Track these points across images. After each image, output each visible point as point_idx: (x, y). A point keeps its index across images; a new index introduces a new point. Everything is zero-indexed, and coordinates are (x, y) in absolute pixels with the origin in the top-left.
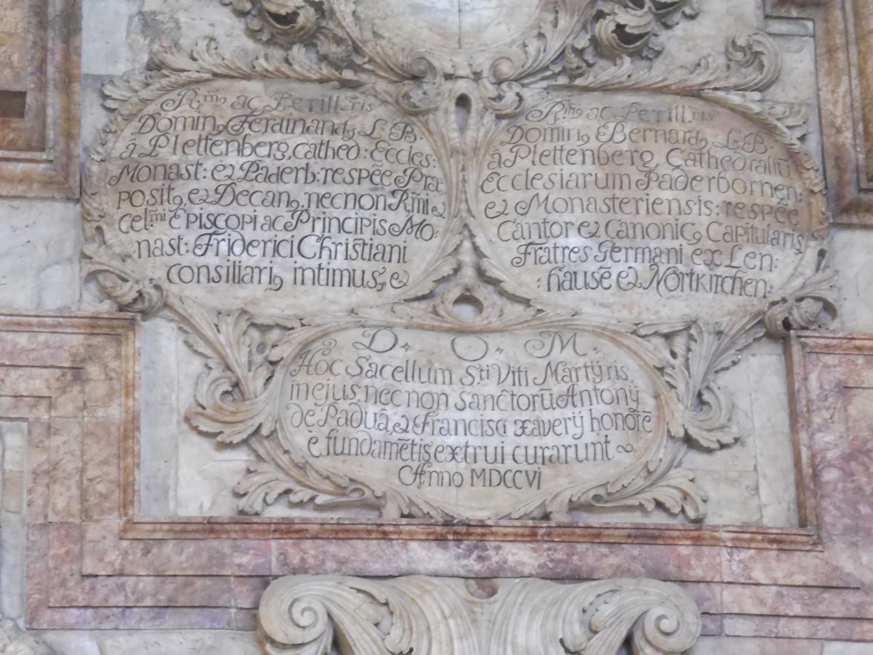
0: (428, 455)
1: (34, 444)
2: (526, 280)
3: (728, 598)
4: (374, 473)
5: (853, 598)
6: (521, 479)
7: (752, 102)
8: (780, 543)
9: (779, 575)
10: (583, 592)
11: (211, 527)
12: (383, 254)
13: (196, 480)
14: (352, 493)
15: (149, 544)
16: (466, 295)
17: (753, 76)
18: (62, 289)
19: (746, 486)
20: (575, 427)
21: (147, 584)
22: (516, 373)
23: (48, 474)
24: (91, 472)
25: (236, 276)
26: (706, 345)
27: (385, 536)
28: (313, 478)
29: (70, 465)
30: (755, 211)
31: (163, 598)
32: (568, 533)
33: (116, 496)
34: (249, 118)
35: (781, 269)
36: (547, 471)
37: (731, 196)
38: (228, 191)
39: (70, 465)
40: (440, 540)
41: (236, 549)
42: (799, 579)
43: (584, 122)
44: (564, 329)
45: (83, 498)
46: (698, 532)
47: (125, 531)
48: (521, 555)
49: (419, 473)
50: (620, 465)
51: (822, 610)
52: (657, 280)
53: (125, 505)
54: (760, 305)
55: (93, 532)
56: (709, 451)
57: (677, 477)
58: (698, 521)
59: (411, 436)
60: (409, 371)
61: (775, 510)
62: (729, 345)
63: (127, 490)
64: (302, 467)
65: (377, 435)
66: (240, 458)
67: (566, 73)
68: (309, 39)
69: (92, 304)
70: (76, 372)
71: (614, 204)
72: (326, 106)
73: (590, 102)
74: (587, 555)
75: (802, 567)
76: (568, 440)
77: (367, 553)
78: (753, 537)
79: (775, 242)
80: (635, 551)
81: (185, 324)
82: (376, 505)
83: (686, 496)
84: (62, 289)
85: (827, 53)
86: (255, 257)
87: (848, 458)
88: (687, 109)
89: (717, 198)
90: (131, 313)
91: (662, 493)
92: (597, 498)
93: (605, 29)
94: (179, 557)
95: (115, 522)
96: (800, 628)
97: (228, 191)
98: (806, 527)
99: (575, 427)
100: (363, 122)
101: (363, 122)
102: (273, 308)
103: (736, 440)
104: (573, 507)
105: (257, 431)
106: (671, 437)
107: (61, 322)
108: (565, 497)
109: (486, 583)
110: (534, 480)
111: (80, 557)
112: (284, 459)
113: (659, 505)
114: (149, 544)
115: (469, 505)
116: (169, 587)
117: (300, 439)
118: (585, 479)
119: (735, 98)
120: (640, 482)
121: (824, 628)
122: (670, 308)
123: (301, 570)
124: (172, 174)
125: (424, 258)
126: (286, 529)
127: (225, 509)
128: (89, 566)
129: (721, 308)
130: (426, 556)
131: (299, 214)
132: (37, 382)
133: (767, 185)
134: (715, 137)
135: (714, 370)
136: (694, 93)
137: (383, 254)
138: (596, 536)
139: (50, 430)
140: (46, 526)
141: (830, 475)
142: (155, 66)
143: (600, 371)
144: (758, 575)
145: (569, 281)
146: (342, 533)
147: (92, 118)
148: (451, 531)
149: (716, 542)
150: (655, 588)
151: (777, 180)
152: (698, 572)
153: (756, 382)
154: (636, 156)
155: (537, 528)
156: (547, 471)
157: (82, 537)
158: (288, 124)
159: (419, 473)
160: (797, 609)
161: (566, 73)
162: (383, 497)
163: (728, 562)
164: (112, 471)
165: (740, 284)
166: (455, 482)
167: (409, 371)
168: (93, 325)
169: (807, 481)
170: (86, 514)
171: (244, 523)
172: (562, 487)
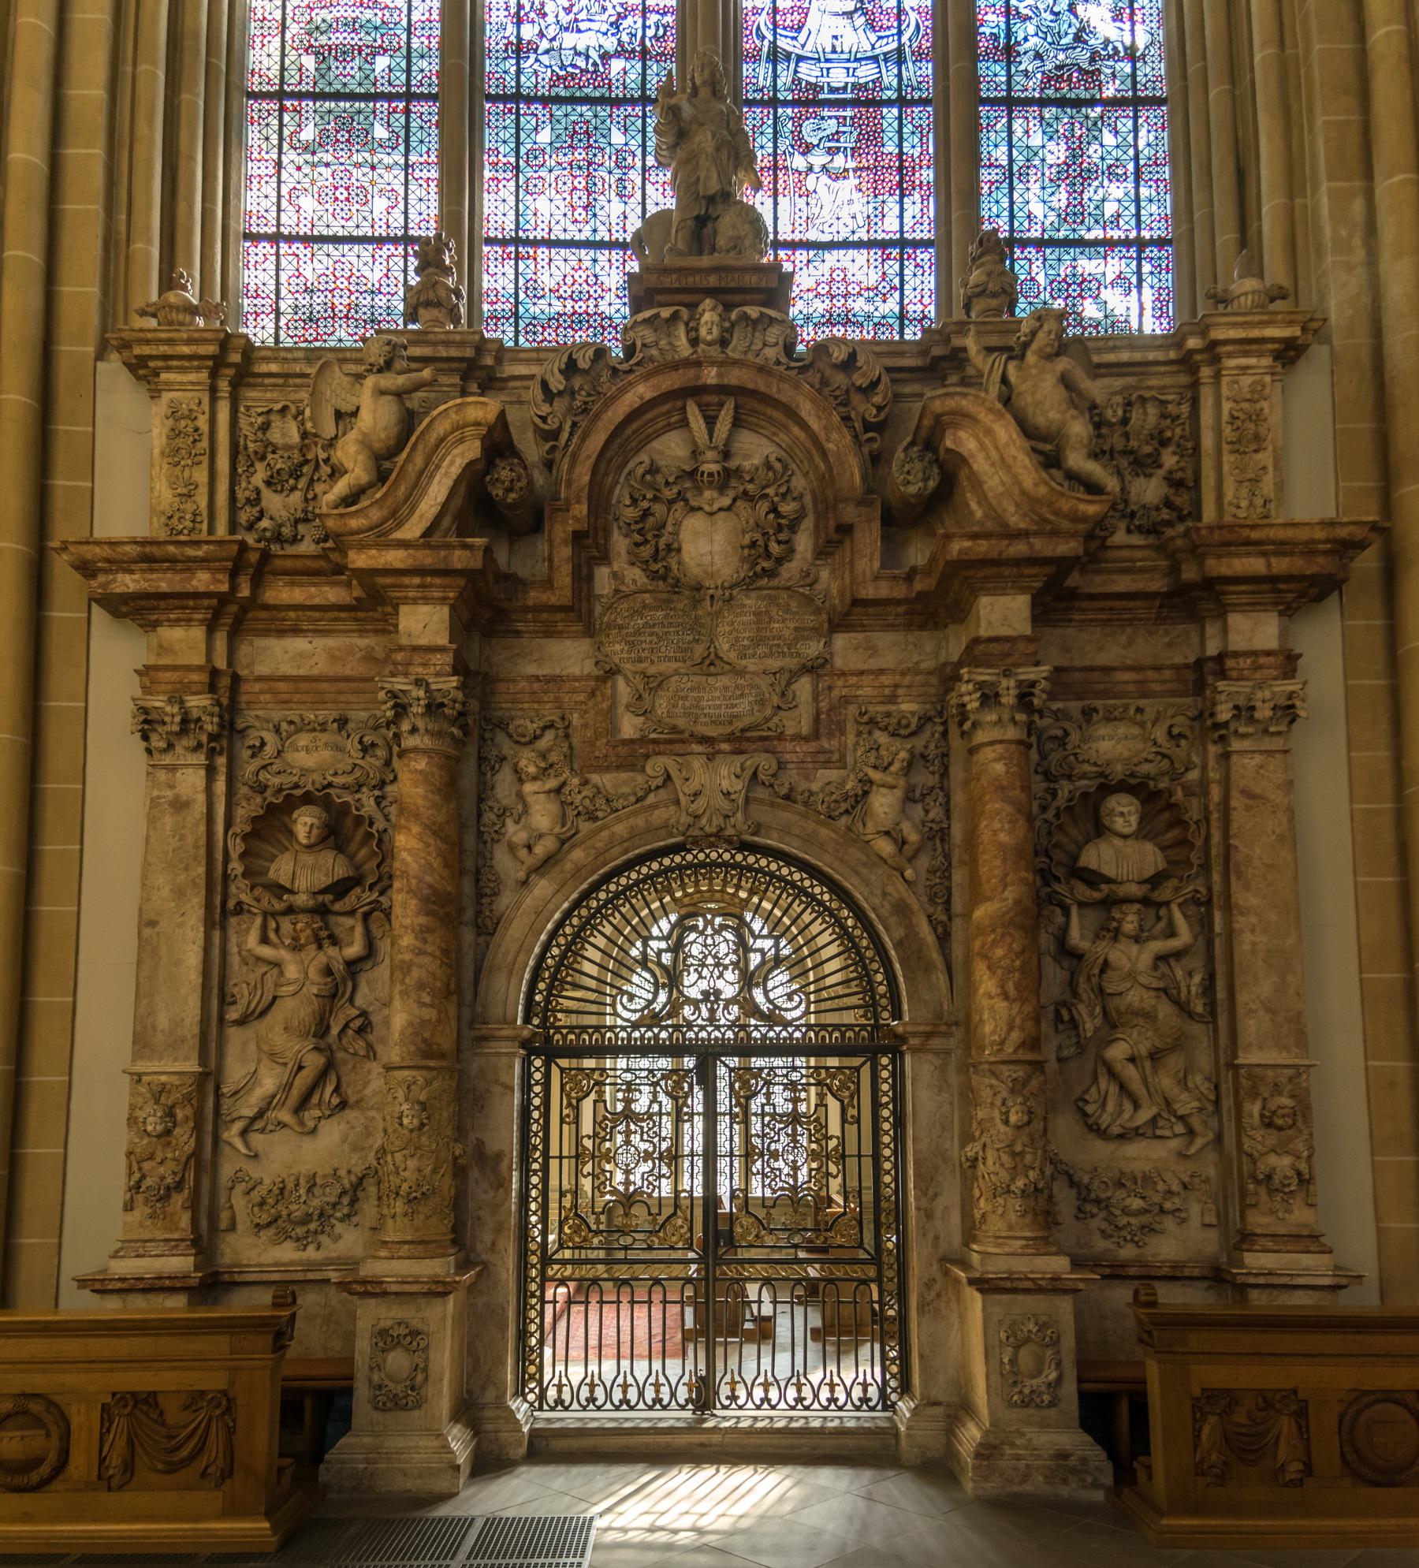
0: (697, 716)
2: (732, 656)
3: (788, 757)
4: (681, 722)
7: (806, 591)
8: (806, 739)
10: (741, 758)
11: (632, 741)
12: (685, 650)
13: (629, 727)
14: (674, 729)
16: (711, 663)
17: (808, 581)
18: (589, 667)
19: (800, 721)
20: (743, 705)
22: (726, 688)
23: (585, 726)
25: (640, 661)
26: (787, 675)
30: (804, 629)
32: (741, 739)
34: (645, 606)
35: (813, 648)
38: (638, 632)
43: (751, 602)
44: (741, 673)
46: (781, 737)
48: (725, 747)
50: (758, 717)
52: (772, 654)
57: (775, 719)
60: (691, 689)
61: (805, 730)
62: (795, 675)
67: (747, 584)
68: (664, 578)
69: (597, 672)
70: (593, 694)
71: (759, 630)
72: (670, 601)
73: (754, 594)
74: (745, 745)
75: (812, 746)
77: (678, 747)
78: (798, 738)
81: (626, 677)
82: (682, 732)
84: (589, 667)
85: (833, 571)
86: (646, 654)
88: (785, 595)
90: (612, 673)
91: (771, 724)
93: (758, 568)
94: (623, 751)
97: (638, 632)
98: (816, 735)
99: (743, 705)
100: (681, 606)
101: (681, 606)
102: (652, 670)
104: (743, 730)
107: (589, 677)
109: (710, 757)
115: (711, 732)
118: (747, 721)
122: (774, 664)
124: (621, 627)
125: (699, 650)
126: (655, 741)
127: (637, 736)
129: (792, 663)
130: (696, 748)
131: (660, 638)
132: (581, 697)
133: (809, 620)
134: (793, 604)
135: (789, 684)
136: (788, 588)
137: (685, 650)
138: (748, 739)
142: (617, 591)
143: (752, 686)
145: (743, 657)
146: (670, 742)
147: (598, 609)
148: (704, 740)
153: (803, 687)
154: (767, 612)
155: (729, 738)
158: (656, 608)
161: (747, 584)
163: (789, 746)
165: (798, 654)
167: (691, 689)
168: (597, 678)
169: (817, 719)
171: (643, 740)
172: (739, 725)
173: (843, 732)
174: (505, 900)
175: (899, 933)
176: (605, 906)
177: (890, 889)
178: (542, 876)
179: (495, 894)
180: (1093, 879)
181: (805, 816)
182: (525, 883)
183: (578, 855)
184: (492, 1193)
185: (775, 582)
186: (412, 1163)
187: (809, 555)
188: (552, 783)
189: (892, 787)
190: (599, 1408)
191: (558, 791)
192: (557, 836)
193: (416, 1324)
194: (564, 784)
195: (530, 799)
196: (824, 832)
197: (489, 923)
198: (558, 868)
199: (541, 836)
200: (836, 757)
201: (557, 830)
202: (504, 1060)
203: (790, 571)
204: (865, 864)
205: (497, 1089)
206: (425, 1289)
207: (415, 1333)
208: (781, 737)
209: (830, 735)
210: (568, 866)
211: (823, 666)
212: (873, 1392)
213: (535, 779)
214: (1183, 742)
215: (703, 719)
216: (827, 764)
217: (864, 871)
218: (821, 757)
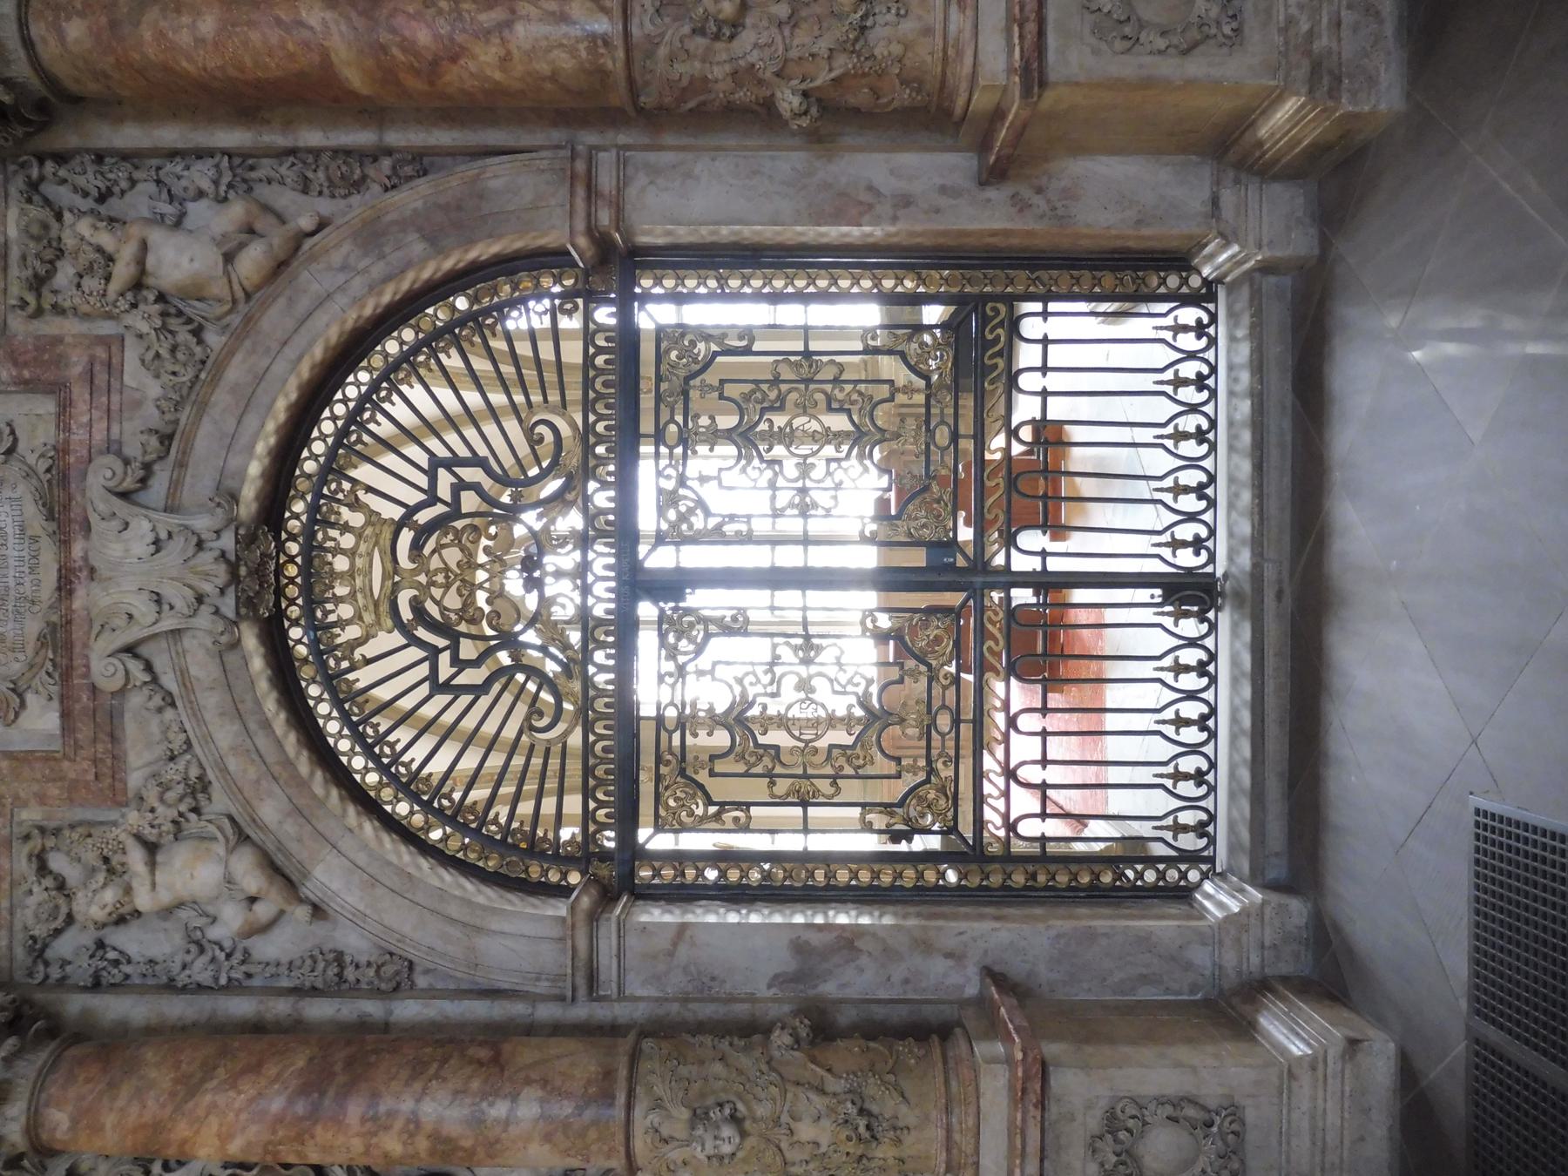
1: (25, 805)
3: (99, 436)
5: (97, 368)
6: (34, 547)
9: (86, 408)
10: (94, 518)
11: (65, 715)
15: (77, 746)
21: (100, 748)
23: (42, 799)
24: (39, 776)
27: (69, 622)
28: (39, 660)
29: (35, 787)
31: (107, 739)
33: (52, 763)
36: (29, 533)
39: (35, 787)
40: (71, 593)
41: (78, 700)
42: (87, 397)
45: (54, 780)
46: (62, 450)
47: (70, 760)
48: (77, 550)
49: (33, 603)
51: (104, 385)
53: (55, 759)
55: (72, 775)
56: (16, 440)
57: (31, 459)
58: (54, 448)
59: (10, 608)
61: (46, 406)
63: (48, 757)
64: (31, 667)
65: (10, 625)
66: (30, 698)
75: (80, 393)
76: (9, 520)
80: (73, 486)
83: (42, 456)
87: (16, 364)
92: (44, 505)
94: (84, 732)
95: (66, 764)
96: (115, 398)
98: (58, 389)
103: (9, 424)
105: (13, 690)
106: (5, 462)
108: (44, 523)
110: (34, 539)
111: (87, 783)
112: (28, 675)
113: (48, 470)
114: (77, 746)
115: (50, 578)
116: (101, 736)
117: (17, 666)
118: (32, 511)
120: (34, 481)
121: (115, 384)
123: (87, 666)
128: (91, 777)
139: (16, 797)
140: (71, 800)
141: (26, 374)
144: (85, 419)
149: (67, 441)
150: (90, 479)
152: (85, 452)
156: (29, 533)
157: (77, 781)
159: (33, 603)
160: (104, 399)
162: (48, 624)
163: (79, 435)
164: (38, 765)
166: (38, 583)
170: (62, 779)
173: (58, 340)
174: (354, 942)
175: (418, 247)
176: (376, 759)
177: (336, 258)
178: (306, 875)
179: (339, 957)
181: (202, 407)
182: (318, 911)
183: (270, 811)
184: (864, 960)
186: (806, 1131)
188: (136, 858)
189: (144, 246)
190: (1213, 765)
191: (152, 848)
192: (230, 851)
193: (1094, 1122)
194: (138, 837)
195: (165, 897)
196: (235, 372)
197: (389, 970)
198: (293, 847)
199: (229, 880)
200: (101, 353)
201: (220, 848)
202: (632, 941)
204: (291, 301)
205: (683, 952)
206: (1035, 1113)
207: (1112, 1123)
208: (62, 450)
209: (60, 361)
210: (290, 828)
212: (1189, 315)
213: (128, 890)
215: (27, 589)
216: (113, 368)
217: (304, 304)
218: (101, 378)
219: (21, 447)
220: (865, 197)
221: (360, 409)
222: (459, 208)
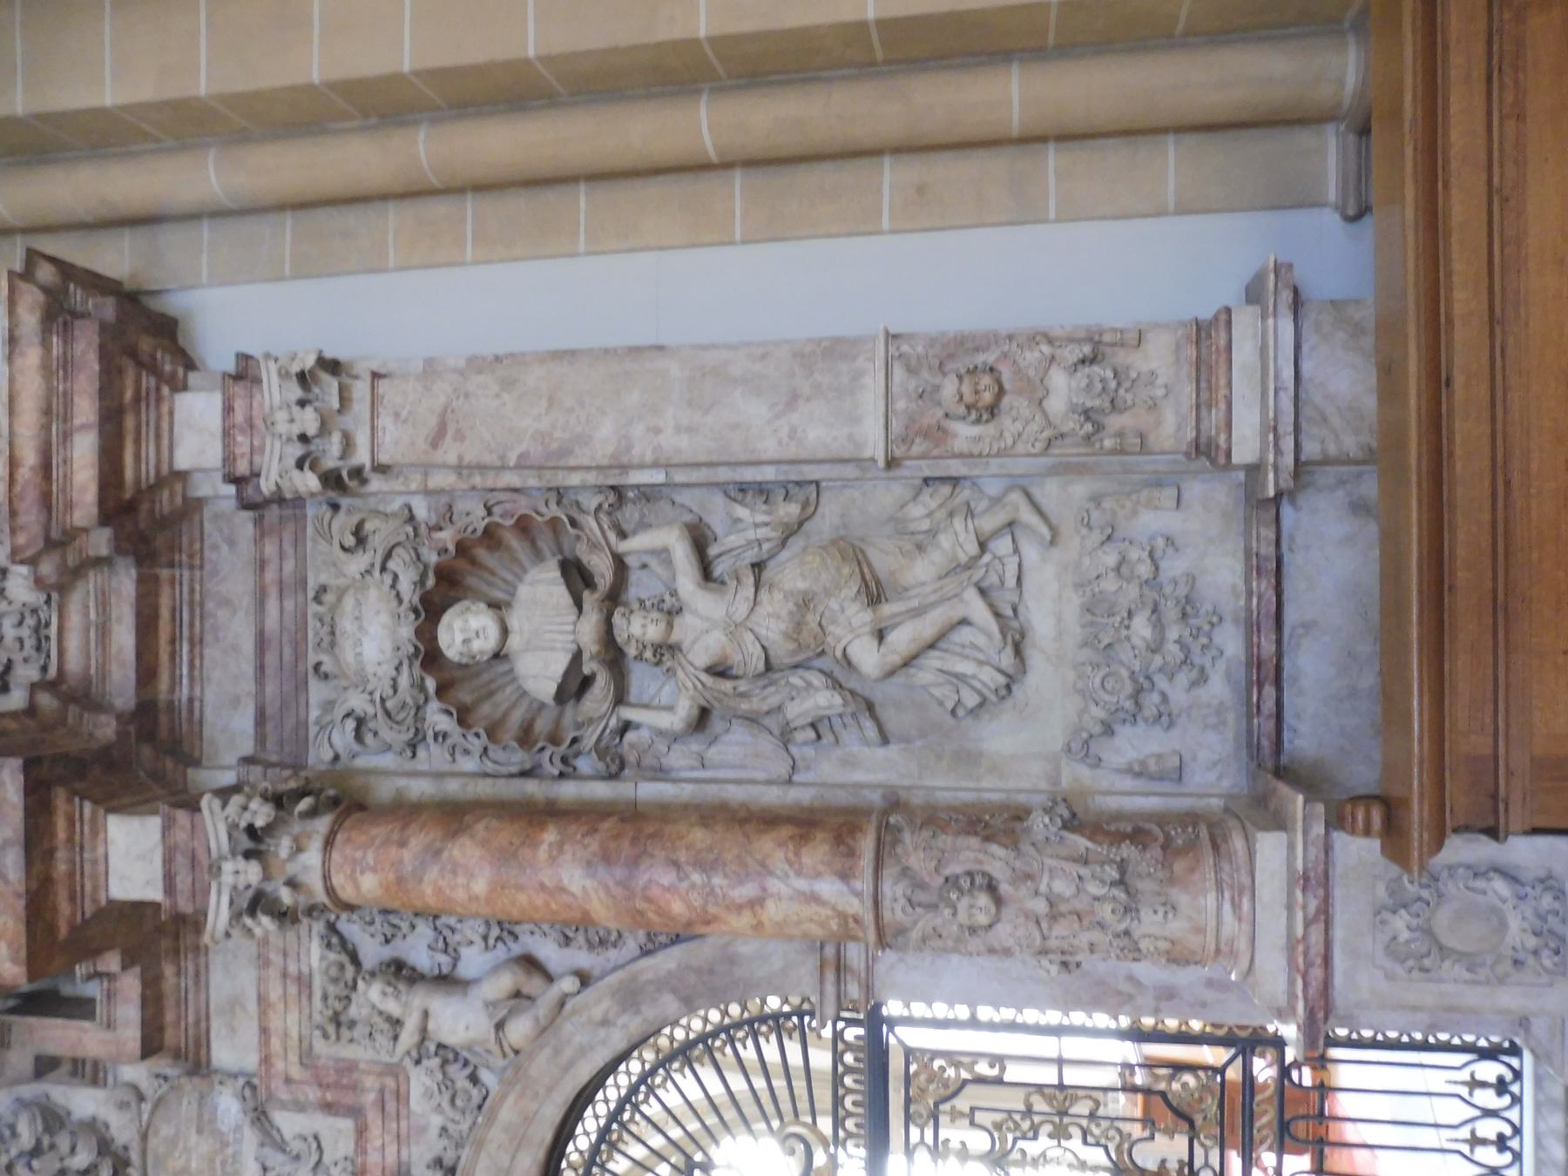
5: (388, 1096)
7: (146, 1107)
30: (200, 1116)
35: (229, 1106)
37: (193, 1130)
51: (394, 1113)
54: (248, 1120)
61: (347, 1124)
75: (373, 1118)
78: (361, 1132)
79: (216, 1108)
87: (320, 1086)
89: (194, 1138)
96: (404, 1124)
98: (355, 1112)
119: (145, 1117)
121: (403, 1112)
129: (250, 1138)
133: (186, 1107)
141: (329, 1097)
144: (378, 1143)
151: (185, 1102)
160: (394, 1125)
165: (238, 1129)
173: (351, 1067)
175: (670, 1004)
177: (597, 1013)
180: (575, 685)
181: (480, 1145)
185: (135, 1156)
187: (99, 1093)
189: (426, 1014)
196: (507, 1114)
200: (390, 1082)
203: (122, 1130)
204: (557, 1052)
209: (354, 1087)
211: (254, 1088)
212: (1489, 1071)
214: (368, 526)
216: (401, 1097)
217: (568, 1053)
218: (391, 1106)
219: (327, 1159)
220: (1125, 987)
221: (620, 1109)
222: (711, 972)
